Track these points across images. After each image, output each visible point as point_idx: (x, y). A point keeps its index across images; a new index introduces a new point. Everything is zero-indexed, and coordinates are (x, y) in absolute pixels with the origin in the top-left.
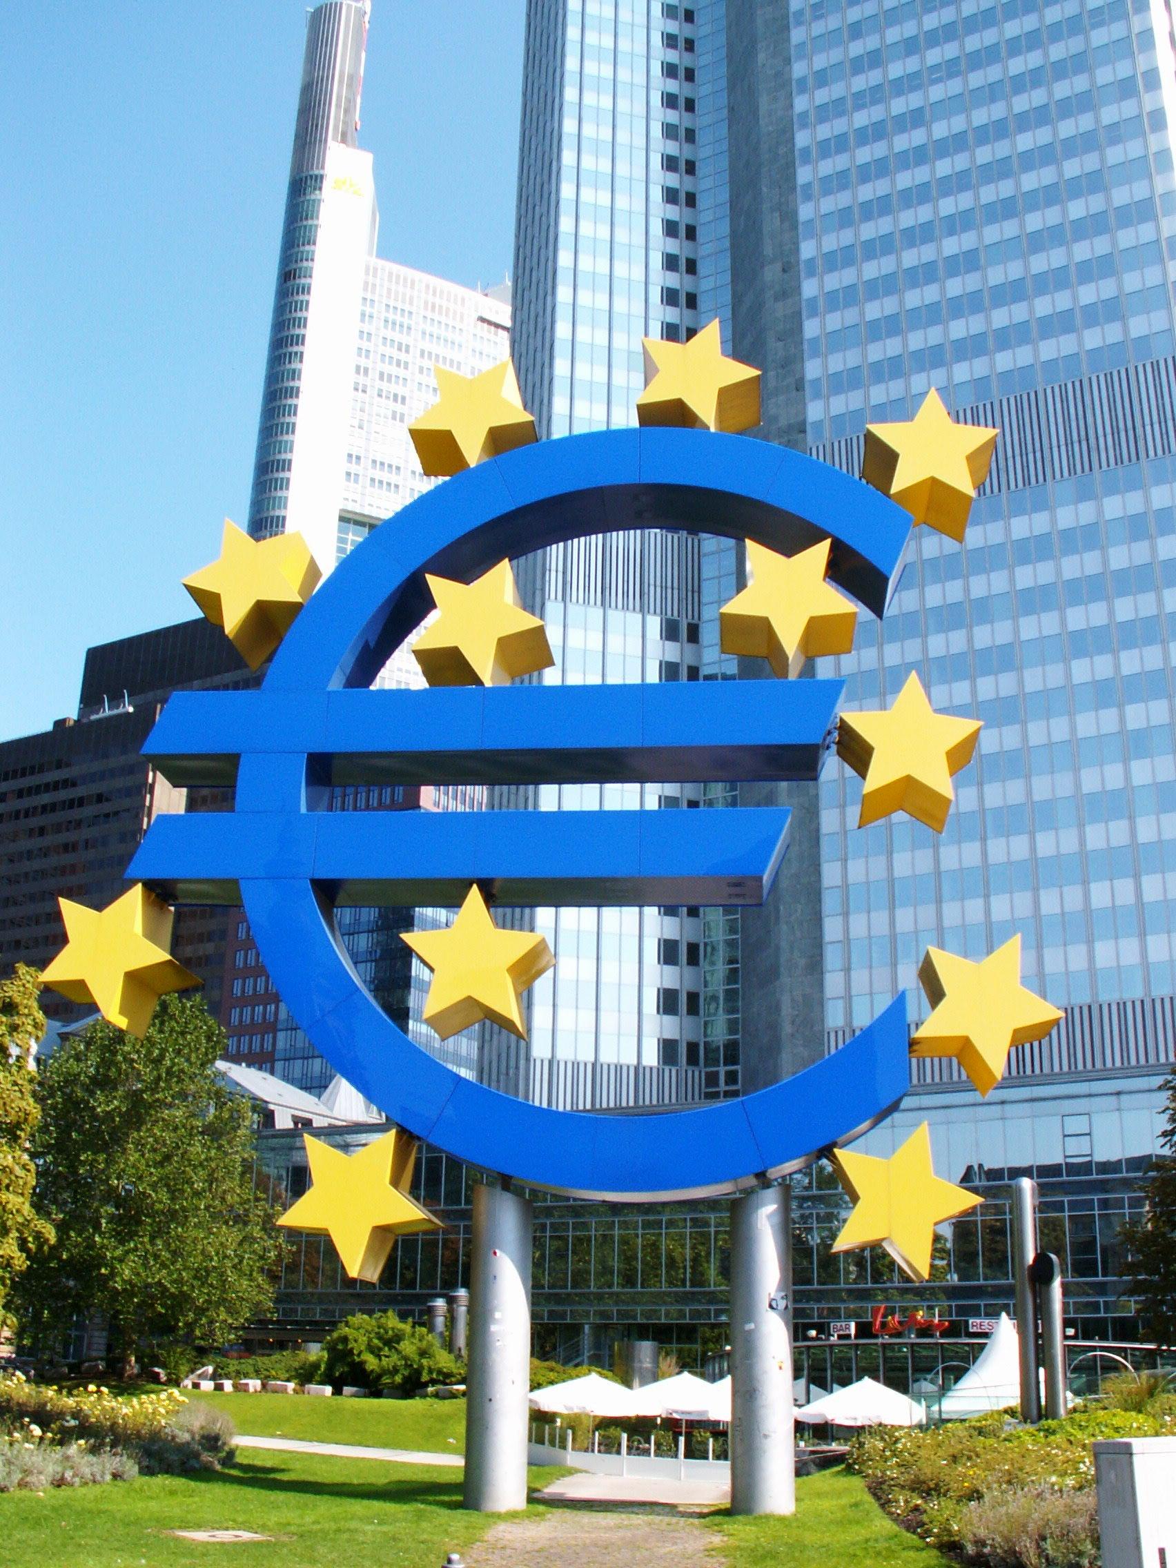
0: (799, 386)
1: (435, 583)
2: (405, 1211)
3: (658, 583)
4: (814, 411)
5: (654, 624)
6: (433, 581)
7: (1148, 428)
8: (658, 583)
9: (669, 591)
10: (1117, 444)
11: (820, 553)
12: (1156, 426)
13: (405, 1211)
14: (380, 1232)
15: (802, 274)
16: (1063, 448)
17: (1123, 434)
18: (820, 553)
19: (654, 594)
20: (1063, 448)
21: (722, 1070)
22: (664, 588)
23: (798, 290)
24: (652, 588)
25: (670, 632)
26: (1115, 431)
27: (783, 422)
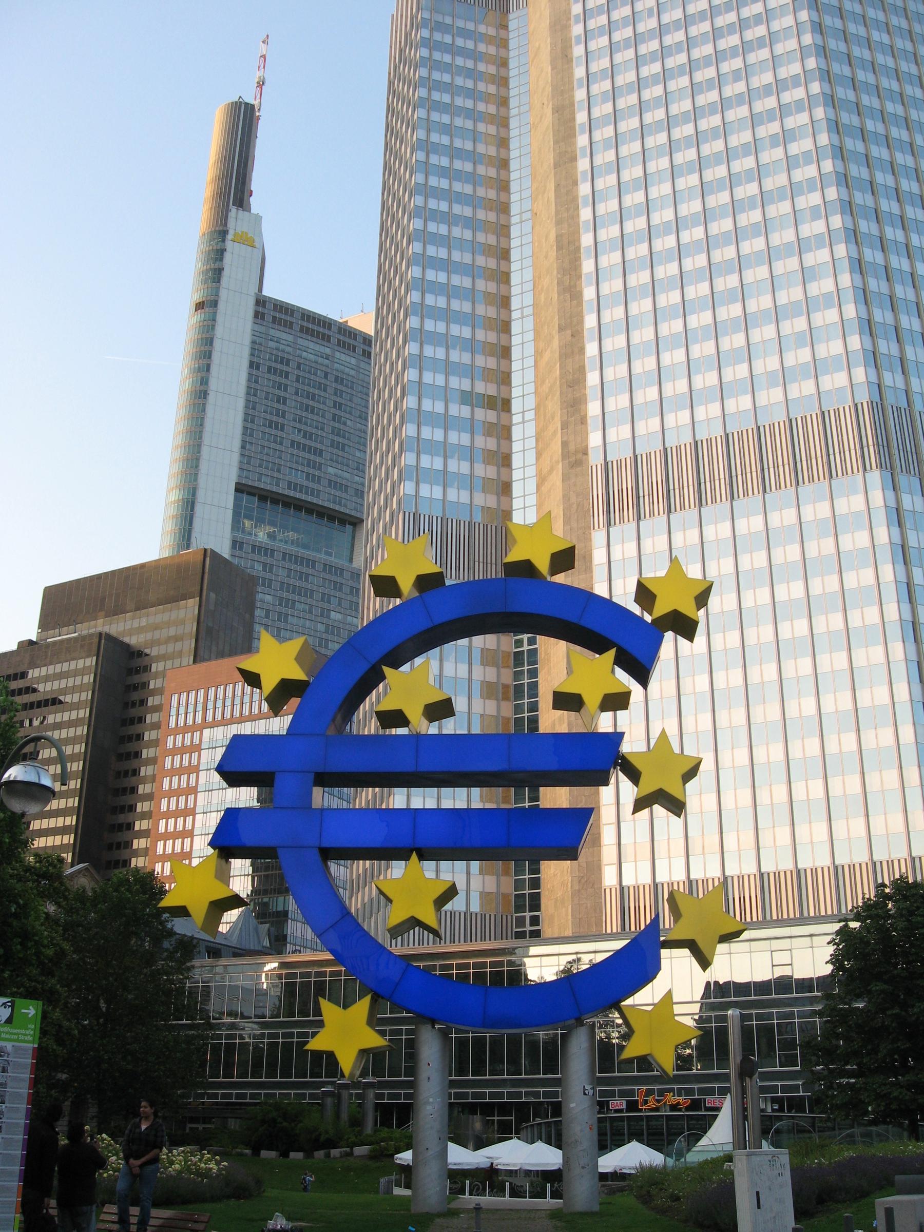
0: (583, 420)
1: (387, 670)
3: (481, 560)
4: (595, 439)
6: (384, 667)
8: (481, 560)
9: (489, 565)
11: (612, 653)
13: (375, 1040)
14: (363, 1052)
16: (772, 470)
18: (612, 653)
20: (772, 470)
21: (528, 915)
23: (582, 350)
24: (477, 564)
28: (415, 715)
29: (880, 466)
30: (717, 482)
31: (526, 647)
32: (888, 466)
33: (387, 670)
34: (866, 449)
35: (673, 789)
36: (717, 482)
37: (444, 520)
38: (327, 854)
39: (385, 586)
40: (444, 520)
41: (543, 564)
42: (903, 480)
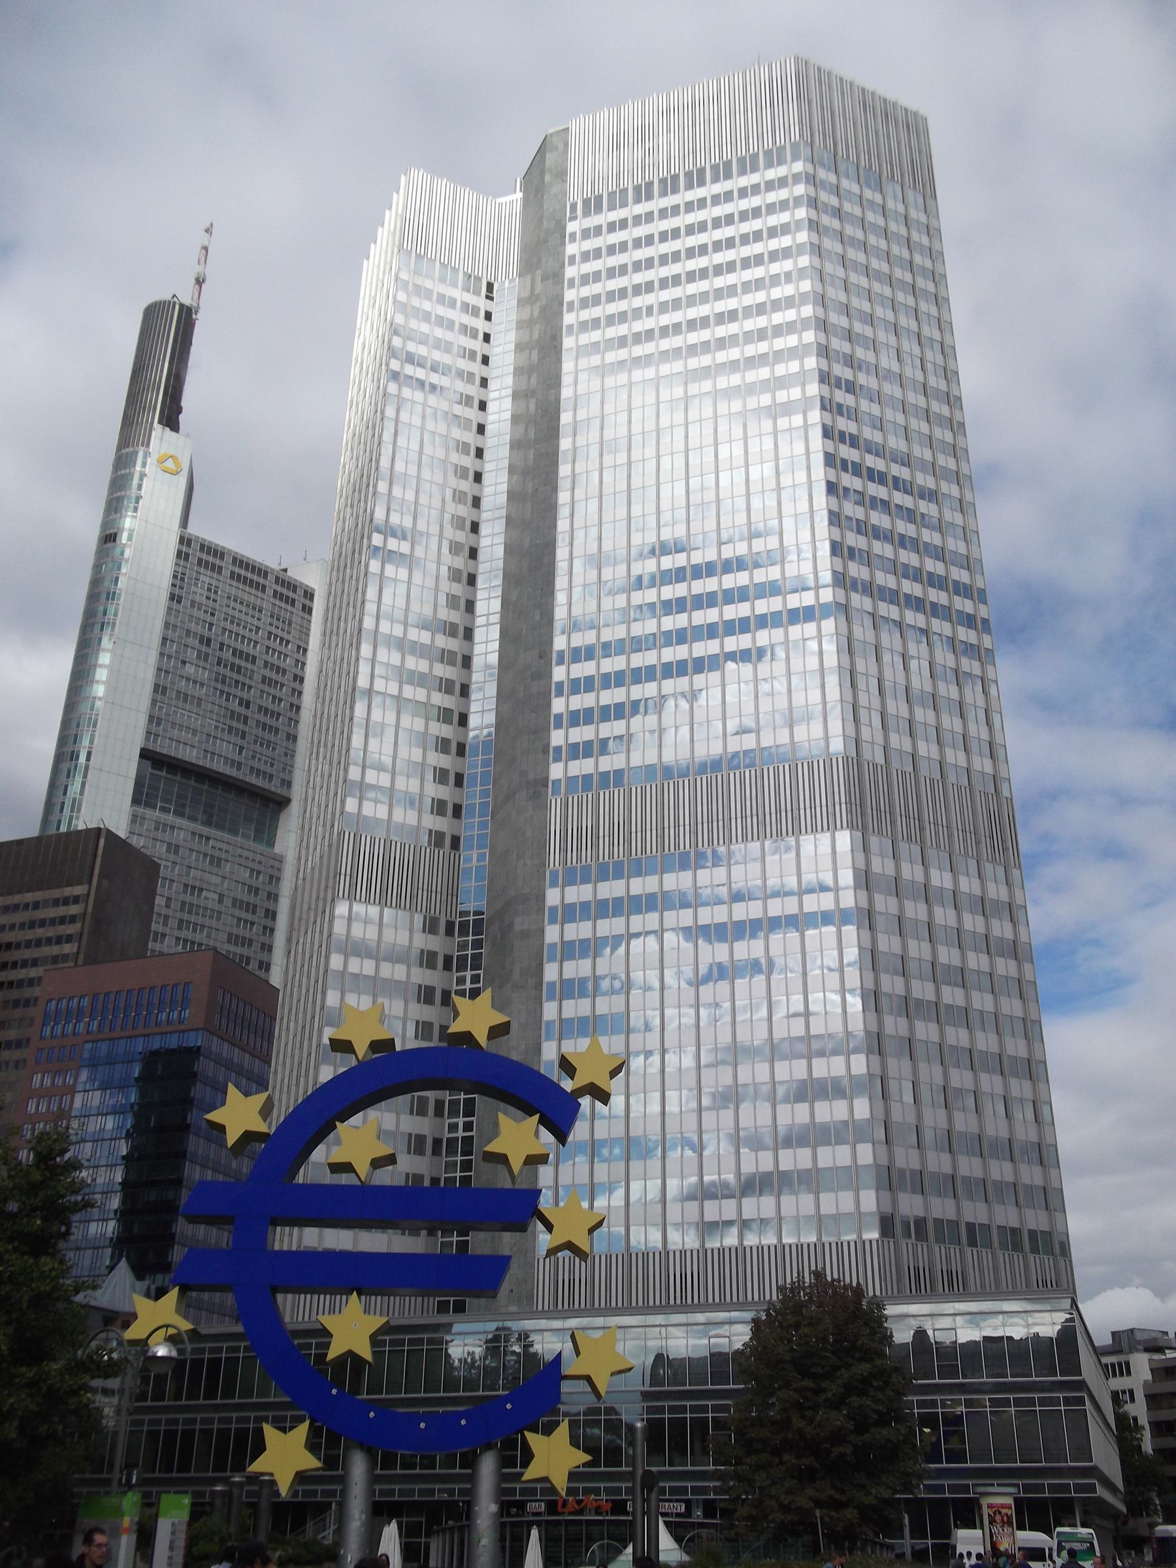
0: (546, 749)
2: (311, 1462)
5: (418, 920)
7: (802, 812)
10: (779, 821)
12: (808, 811)
13: (311, 1462)
15: (554, 663)
16: (739, 820)
17: (783, 814)
19: (423, 896)
20: (739, 820)
22: (430, 891)
23: (549, 675)
25: (431, 927)
26: (778, 811)
27: (531, 777)
28: (363, 1168)
29: (851, 826)
30: (681, 828)
31: (460, 1133)
32: (860, 823)
33: (338, 1123)
34: (837, 807)
35: (583, 1243)
36: (681, 828)
37: (388, 843)
38: (275, 1290)
39: (341, 1046)
40: (388, 843)
41: (482, 1038)
42: (874, 841)
